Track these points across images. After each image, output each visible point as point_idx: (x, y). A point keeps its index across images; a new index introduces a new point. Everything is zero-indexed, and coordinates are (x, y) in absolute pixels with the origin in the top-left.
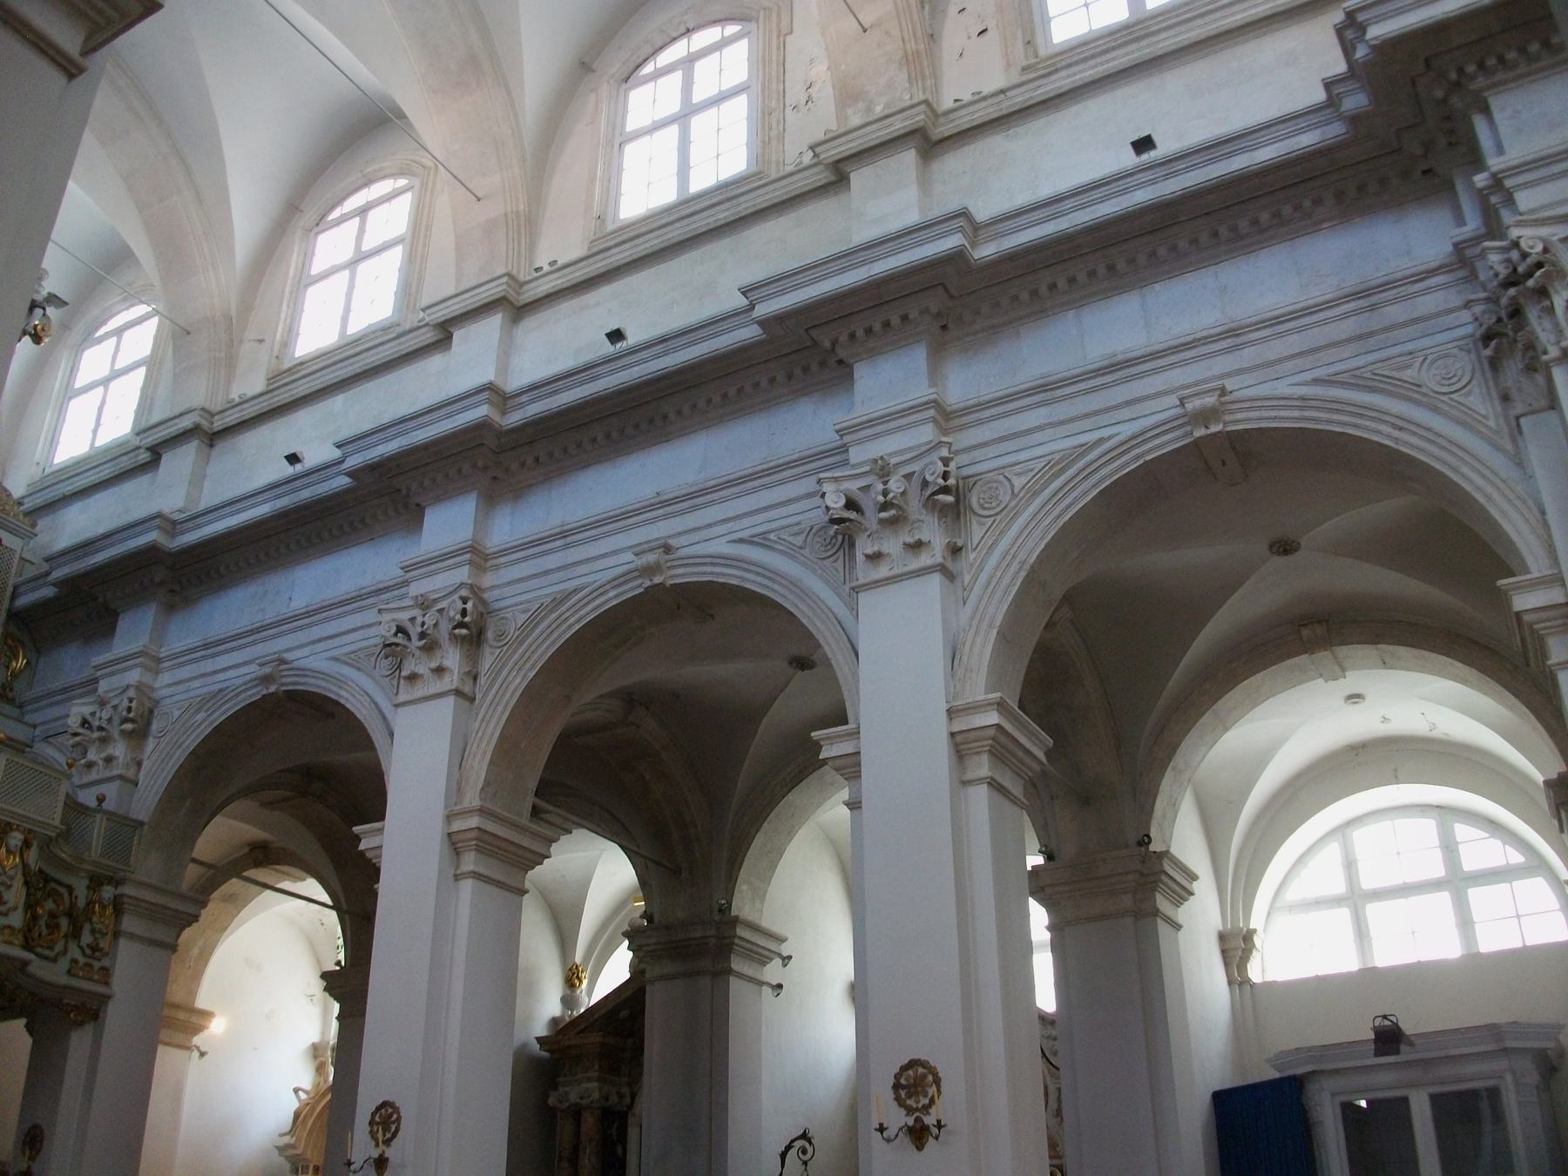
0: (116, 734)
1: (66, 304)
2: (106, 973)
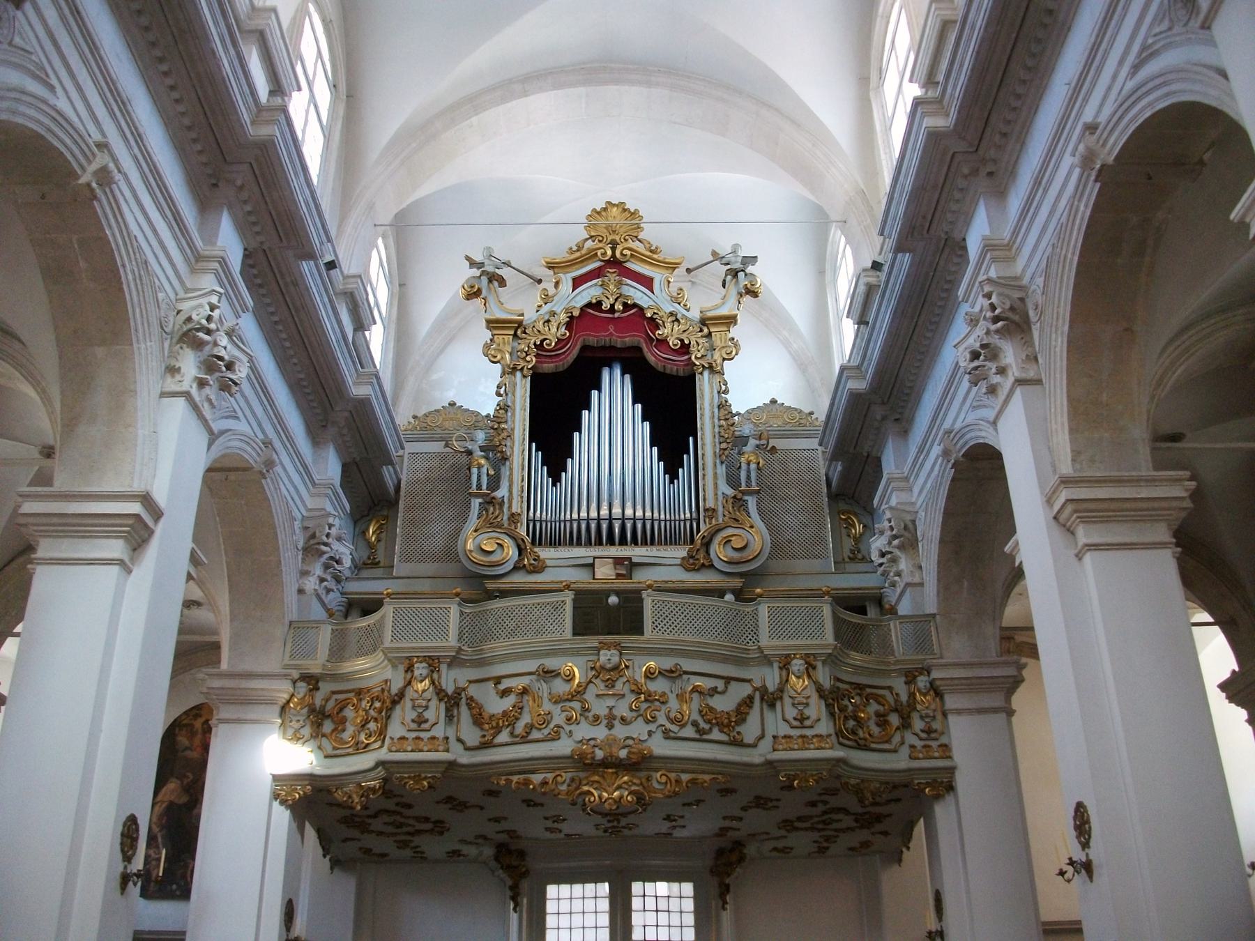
1: (756, 257)
2: (945, 747)
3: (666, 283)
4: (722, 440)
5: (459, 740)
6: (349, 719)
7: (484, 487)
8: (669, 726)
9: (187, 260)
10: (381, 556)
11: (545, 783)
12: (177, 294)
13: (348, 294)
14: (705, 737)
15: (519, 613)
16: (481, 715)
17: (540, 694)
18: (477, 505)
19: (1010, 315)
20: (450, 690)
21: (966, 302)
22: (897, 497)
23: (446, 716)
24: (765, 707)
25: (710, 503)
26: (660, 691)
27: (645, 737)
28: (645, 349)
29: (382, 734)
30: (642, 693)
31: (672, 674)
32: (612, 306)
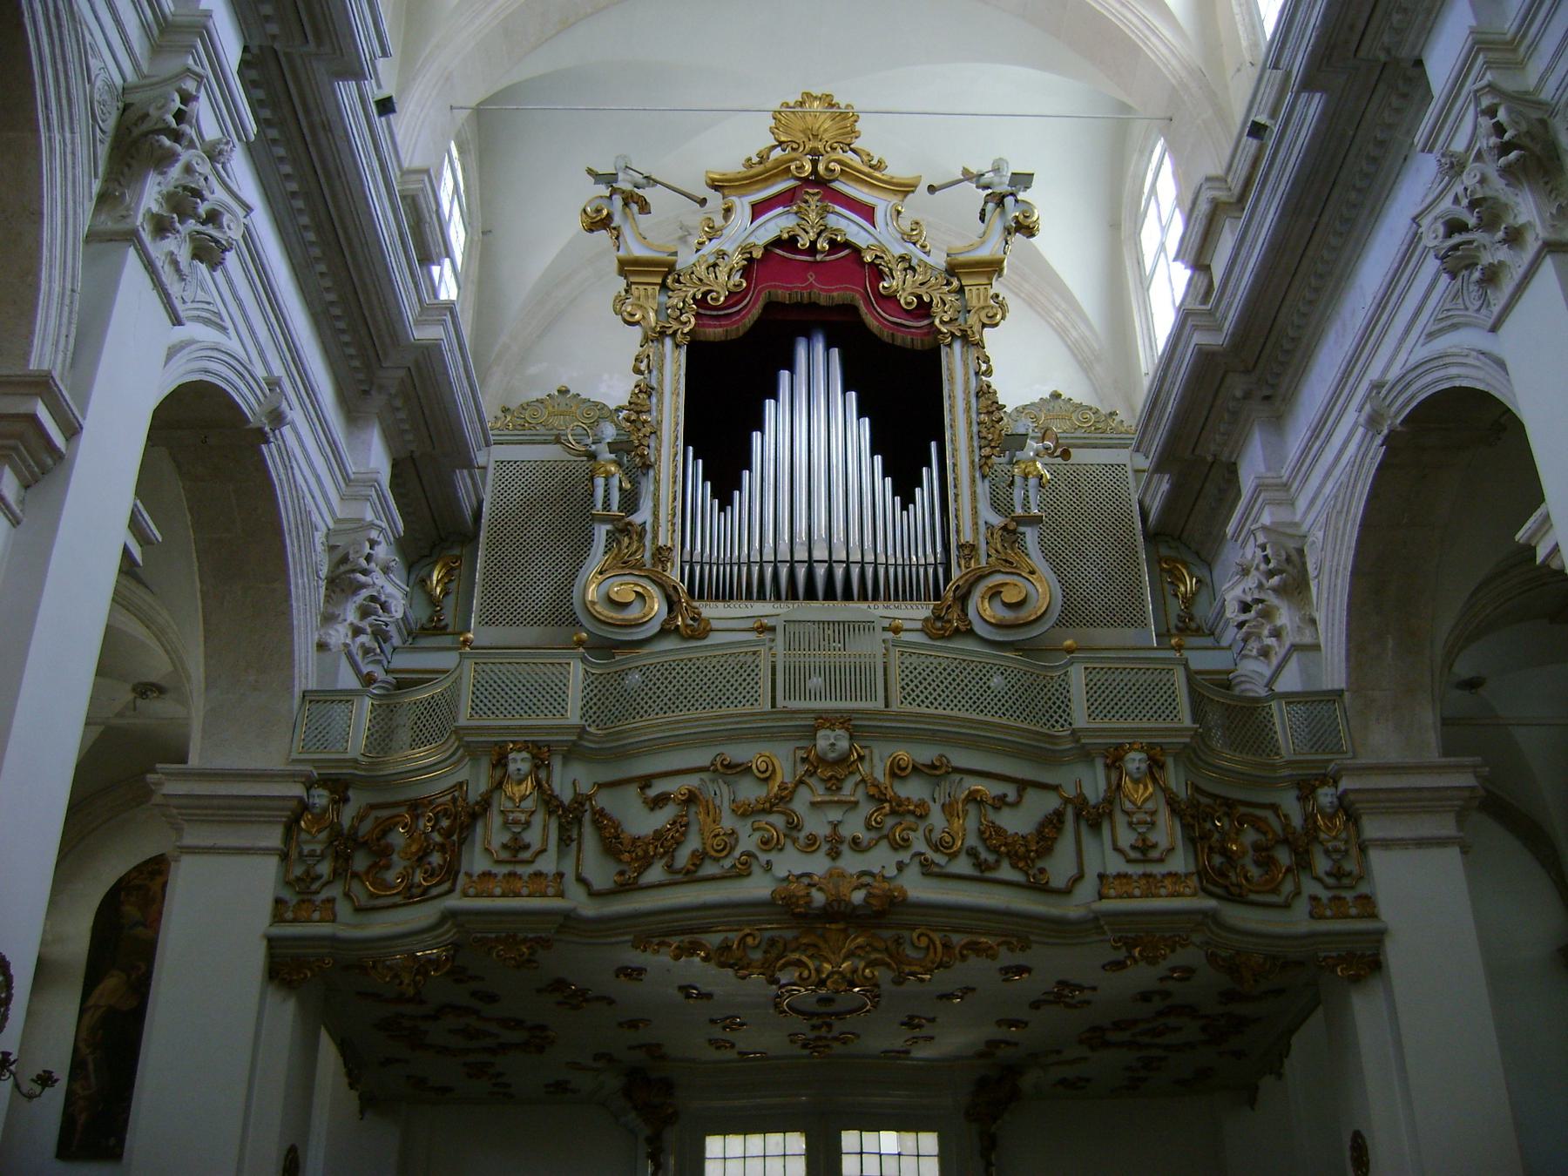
0: (1272, 599)
2: (1367, 905)
3: (895, 214)
4: (983, 442)
5: (581, 880)
6: (397, 849)
7: (615, 506)
8: (931, 854)
9: (145, 27)
10: (449, 617)
11: (725, 948)
12: (124, 80)
13: (409, 201)
14: (988, 875)
15: (682, 673)
16: (617, 837)
17: (718, 802)
18: (604, 537)
19: (1526, 141)
20: (567, 797)
21: (1430, 151)
22: (1272, 514)
23: (561, 839)
24: (1084, 829)
25: (967, 536)
26: (915, 797)
27: (891, 871)
28: (863, 309)
29: (450, 872)
30: (886, 801)
31: (933, 772)
32: (813, 243)
